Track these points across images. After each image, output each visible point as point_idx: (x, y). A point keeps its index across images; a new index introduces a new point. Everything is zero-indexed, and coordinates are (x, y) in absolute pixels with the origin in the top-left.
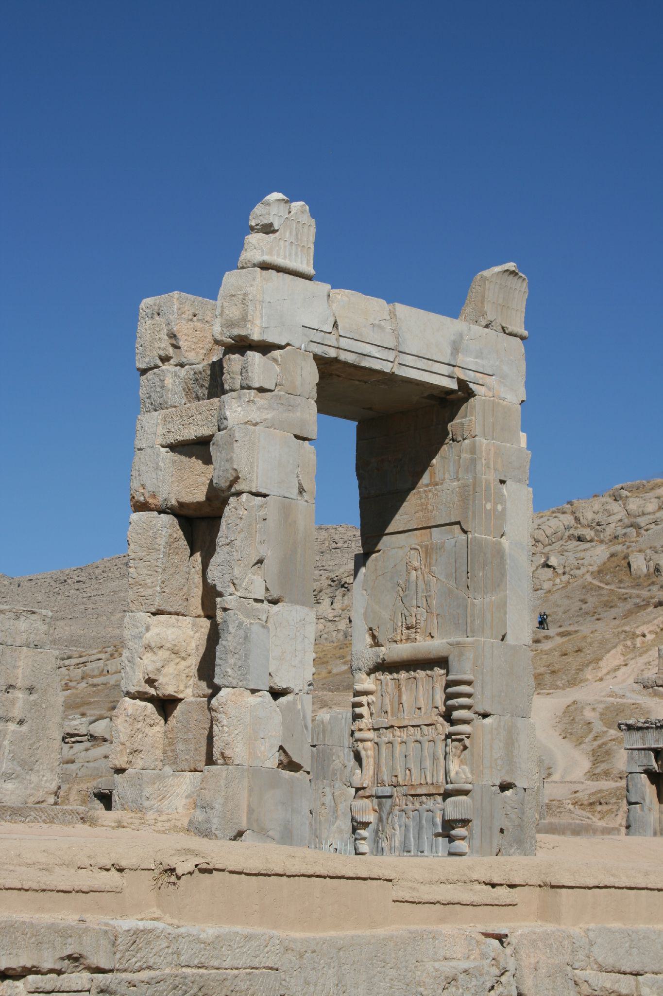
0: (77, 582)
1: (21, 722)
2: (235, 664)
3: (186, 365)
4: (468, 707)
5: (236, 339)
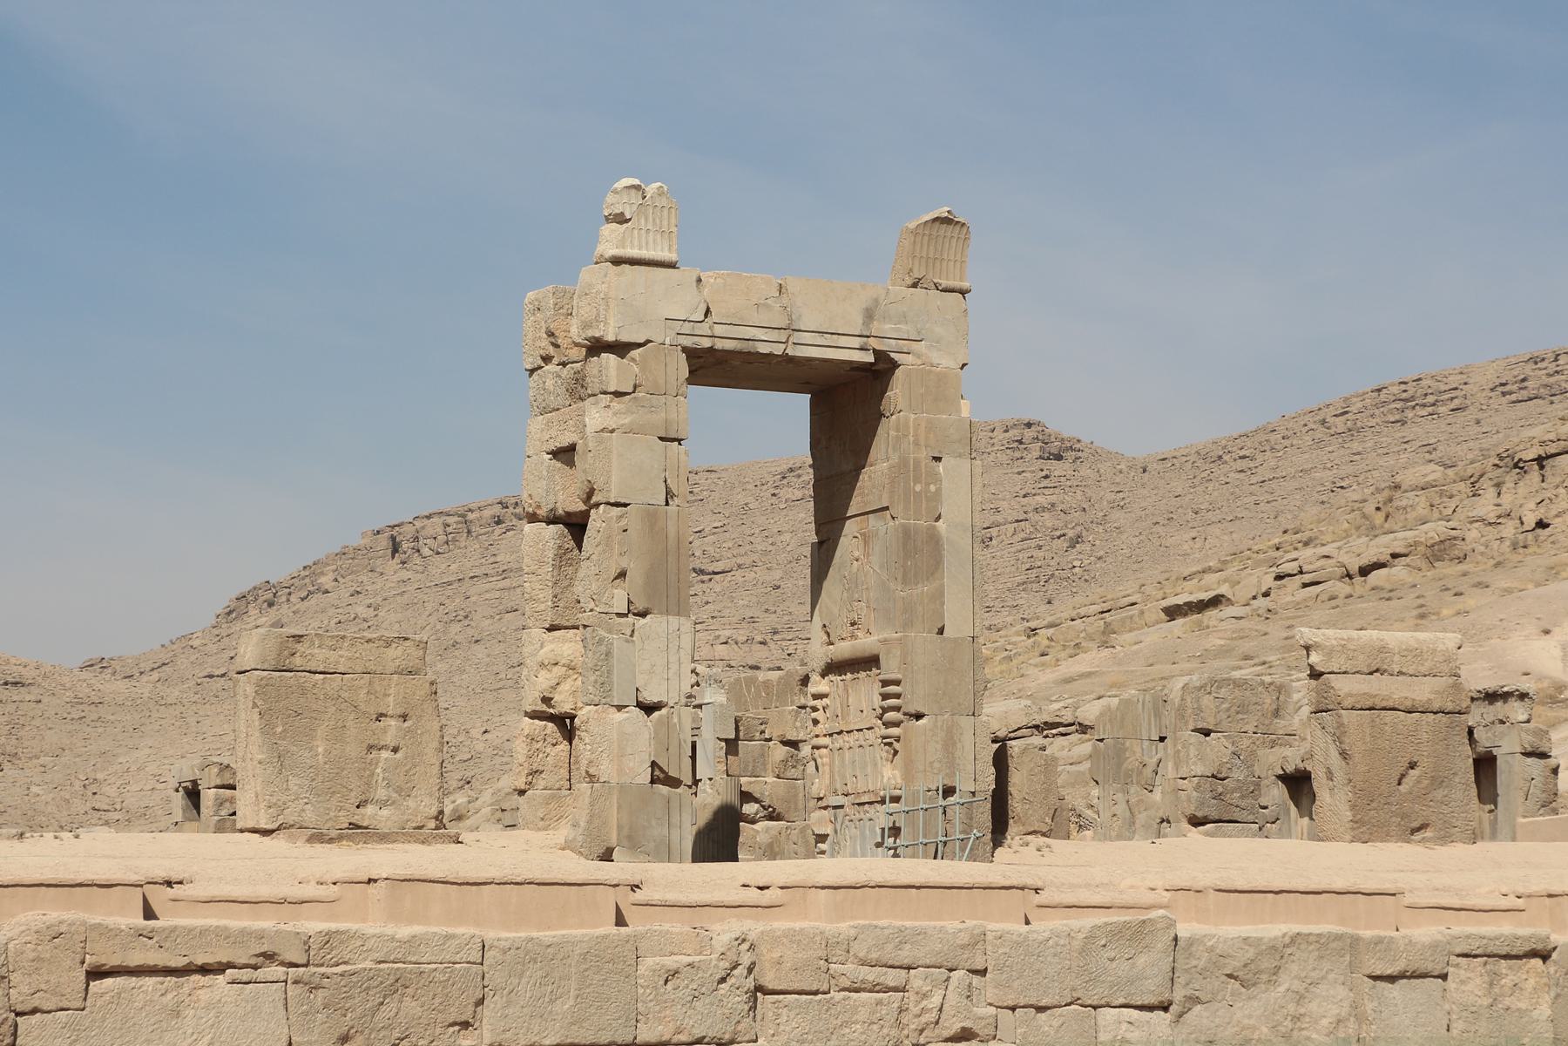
0: (1241, 458)
1: (395, 750)
2: (596, 682)
3: (568, 364)
4: (897, 709)
5: (592, 340)
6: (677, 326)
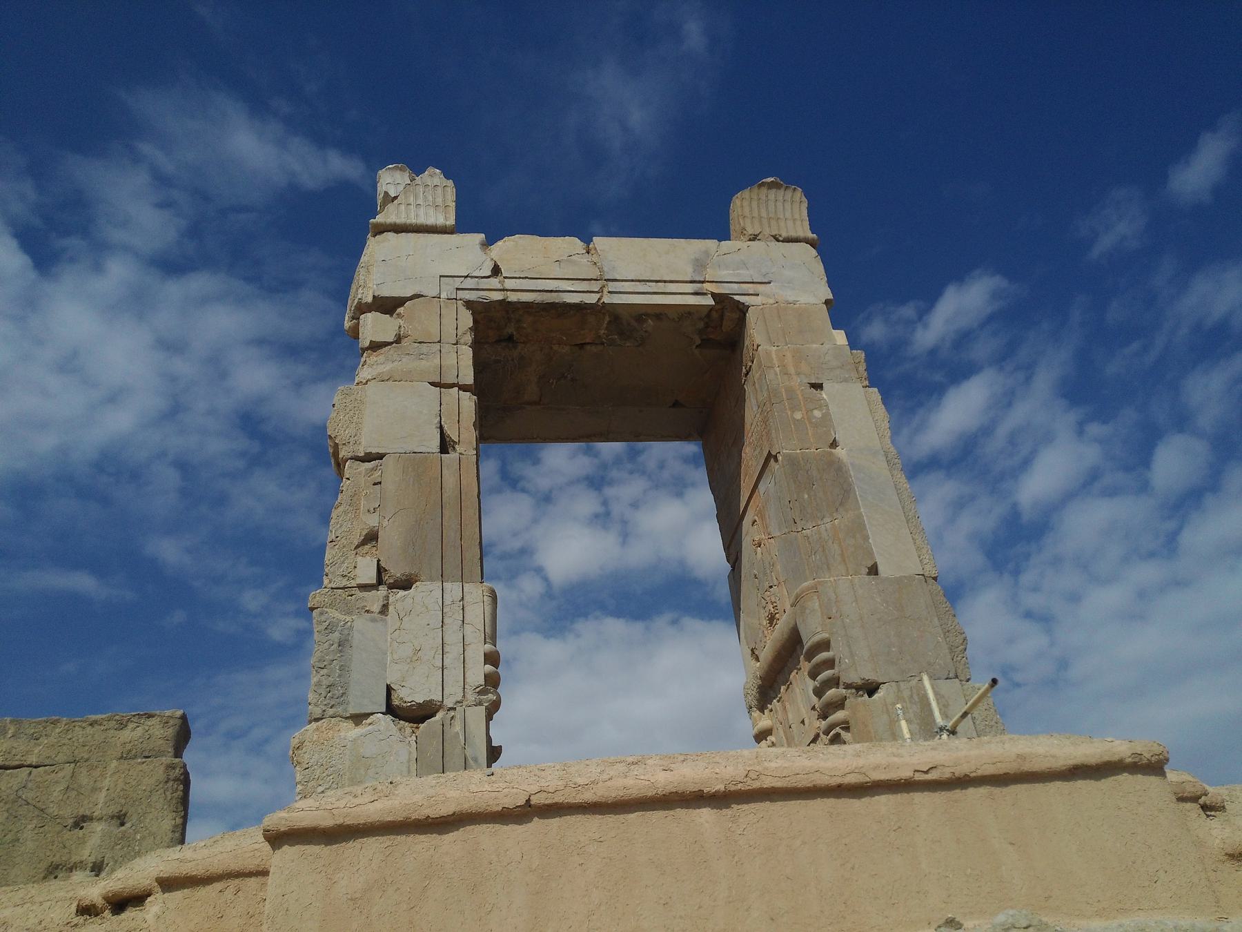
6: (458, 283)
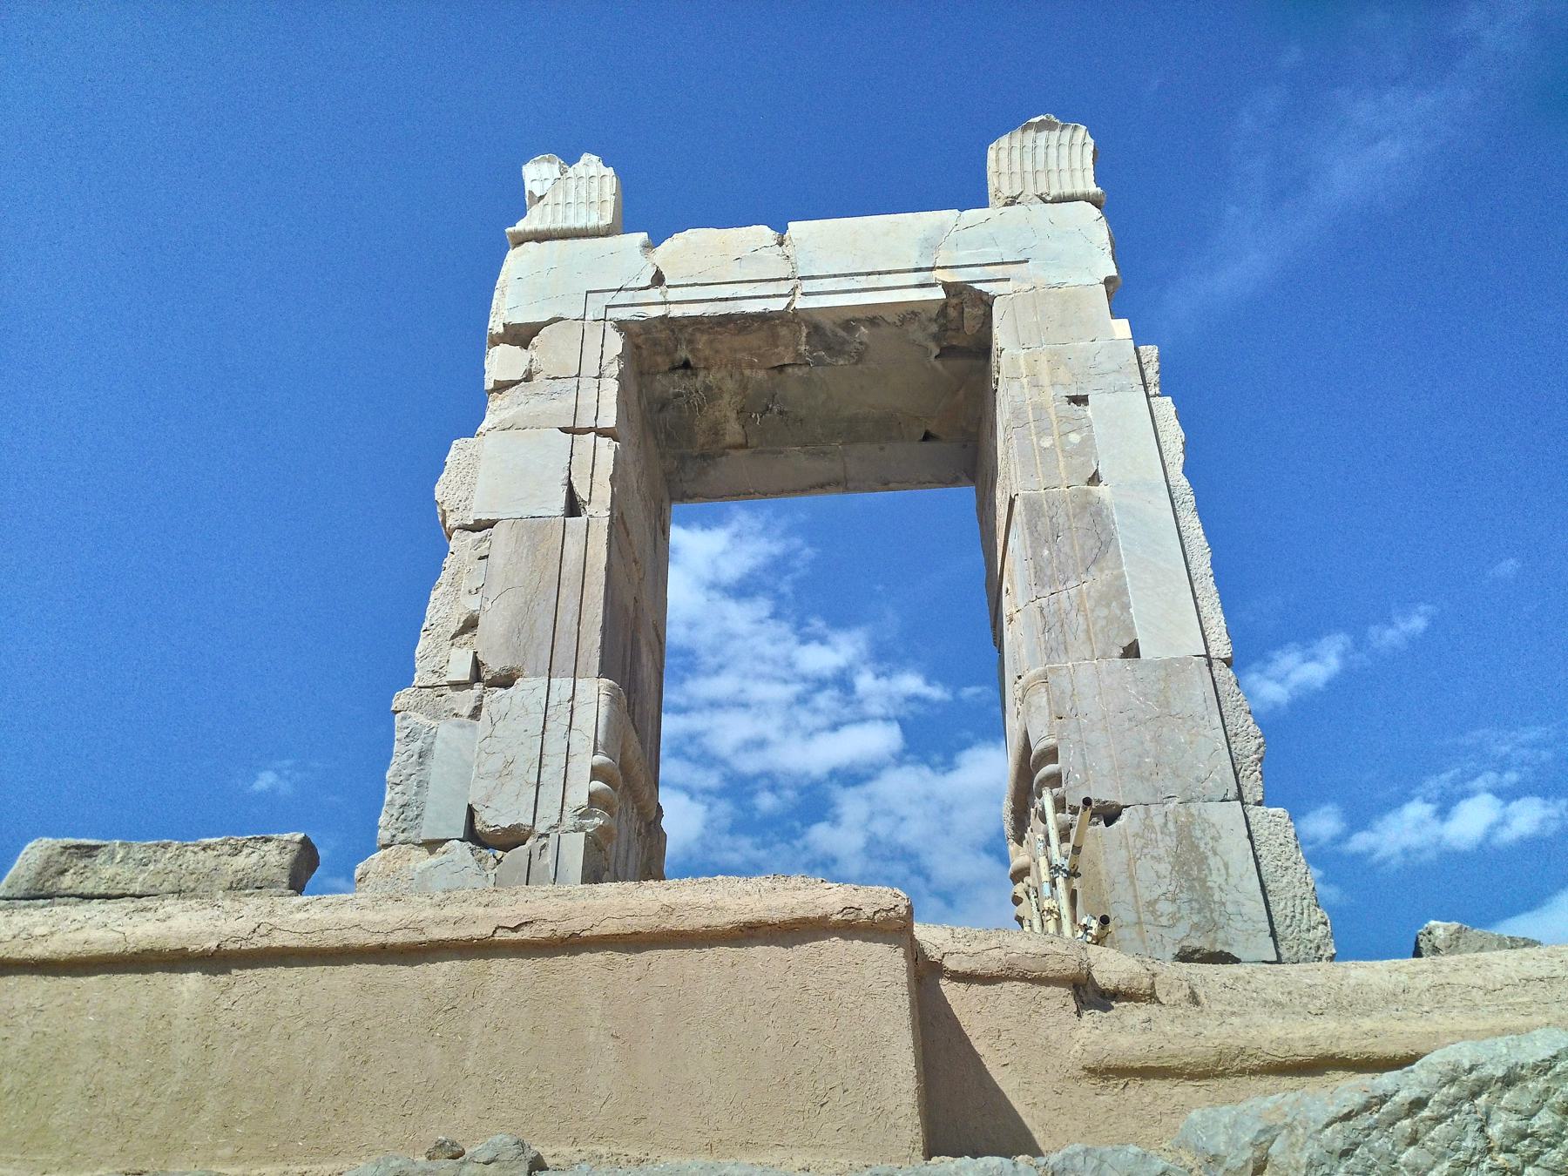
6: (608, 299)
